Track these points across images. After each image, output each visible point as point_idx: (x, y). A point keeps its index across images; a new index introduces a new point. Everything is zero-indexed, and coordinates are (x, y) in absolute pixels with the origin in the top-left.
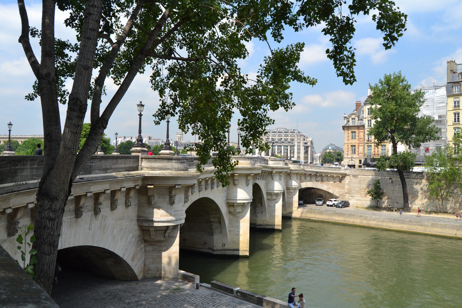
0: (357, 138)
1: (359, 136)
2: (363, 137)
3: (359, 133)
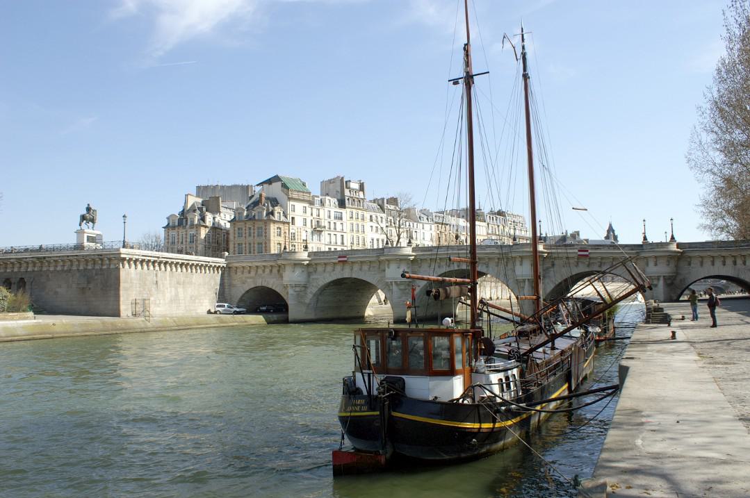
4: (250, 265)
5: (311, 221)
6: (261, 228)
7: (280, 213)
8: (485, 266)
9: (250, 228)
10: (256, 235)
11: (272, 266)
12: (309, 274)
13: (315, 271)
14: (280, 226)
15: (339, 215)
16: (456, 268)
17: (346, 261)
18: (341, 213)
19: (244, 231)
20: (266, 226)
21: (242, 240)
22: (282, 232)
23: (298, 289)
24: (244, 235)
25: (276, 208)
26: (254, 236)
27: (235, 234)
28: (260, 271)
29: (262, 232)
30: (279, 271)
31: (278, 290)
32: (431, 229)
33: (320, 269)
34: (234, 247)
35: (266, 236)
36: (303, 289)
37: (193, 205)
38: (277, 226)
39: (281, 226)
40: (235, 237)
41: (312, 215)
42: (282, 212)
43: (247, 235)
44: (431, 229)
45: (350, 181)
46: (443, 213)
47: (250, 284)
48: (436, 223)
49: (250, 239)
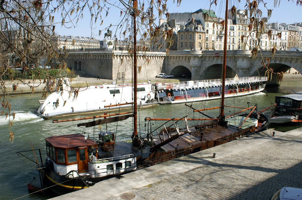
0: (201, 39)
1: (202, 38)
2: (204, 39)
3: (202, 36)
4: (176, 55)
5: (217, 31)
6: (192, 35)
7: (201, 28)
8: (289, 62)
9: (186, 35)
10: (189, 39)
11: (186, 57)
12: (202, 61)
13: (205, 60)
14: (200, 34)
15: (232, 28)
16: (273, 62)
17: (218, 56)
18: (234, 27)
19: (184, 37)
20: (193, 34)
21: (182, 41)
22: (202, 37)
23: (196, 68)
24: (184, 38)
25: (199, 26)
26: (188, 39)
27: (180, 38)
28: (181, 59)
29: (192, 37)
30: (189, 59)
31: (188, 68)
32: (286, 34)
33: (207, 59)
34: (179, 44)
35: (193, 39)
36: (199, 68)
37: (163, 24)
38: (199, 34)
39: (201, 34)
40: (179, 39)
41: (217, 28)
42: (202, 28)
43: (185, 38)
44: (286, 34)
45: (240, 10)
46: (294, 25)
47: (177, 65)
48: (289, 31)
49: (186, 41)
